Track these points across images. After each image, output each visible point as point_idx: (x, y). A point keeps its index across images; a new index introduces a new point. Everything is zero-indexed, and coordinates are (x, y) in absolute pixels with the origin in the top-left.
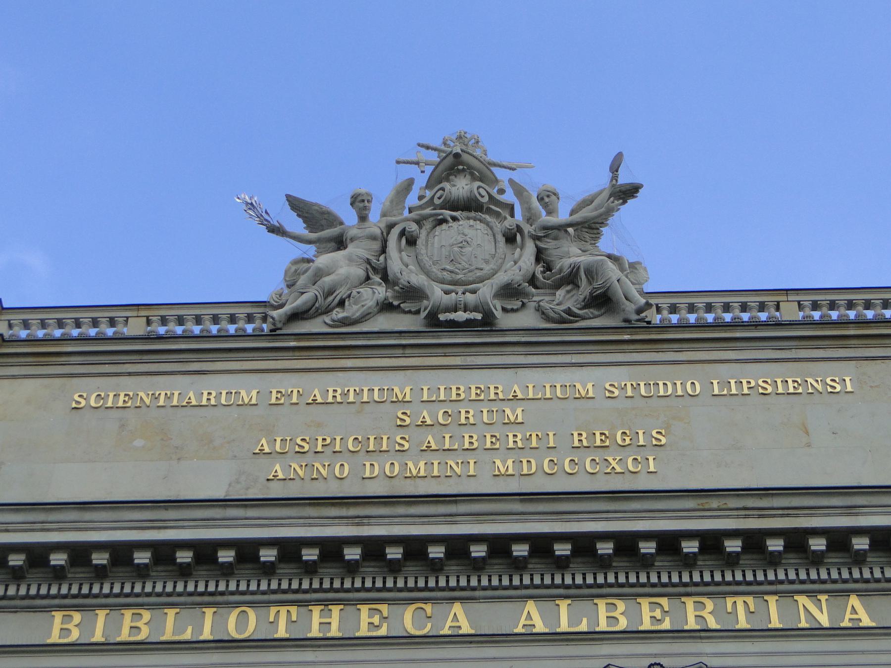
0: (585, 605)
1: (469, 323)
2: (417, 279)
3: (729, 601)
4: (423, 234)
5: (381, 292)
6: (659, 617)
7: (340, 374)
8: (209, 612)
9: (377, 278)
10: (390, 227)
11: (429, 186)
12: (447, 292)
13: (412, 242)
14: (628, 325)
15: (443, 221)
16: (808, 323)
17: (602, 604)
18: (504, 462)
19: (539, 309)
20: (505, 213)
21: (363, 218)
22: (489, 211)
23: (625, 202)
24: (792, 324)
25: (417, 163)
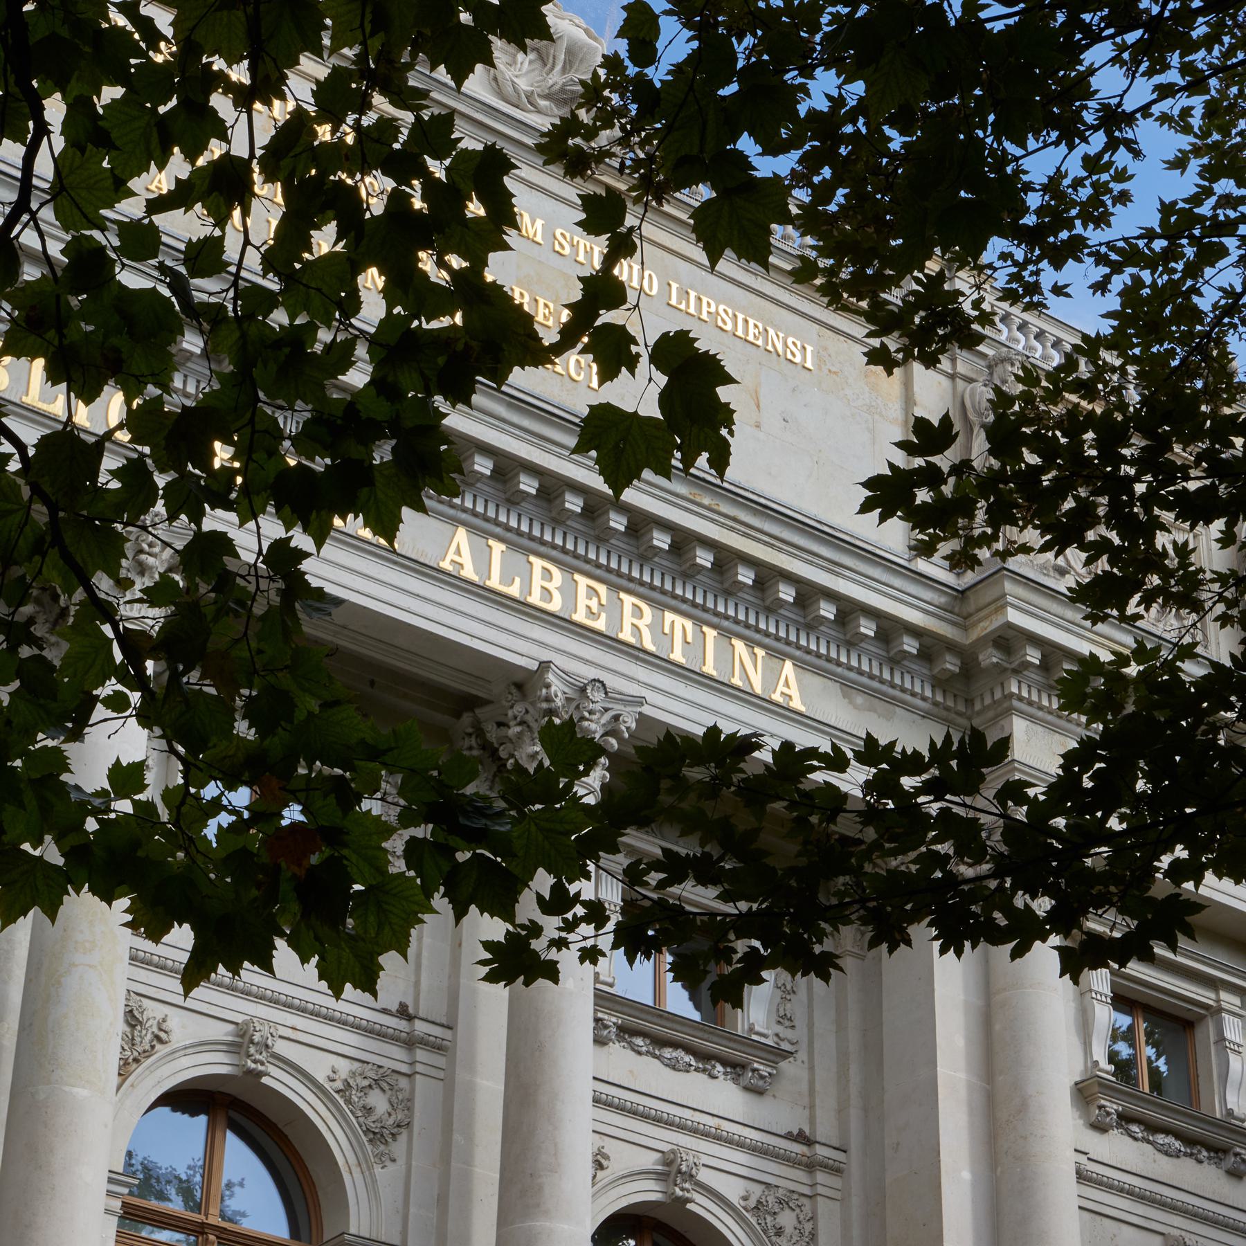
0: (519, 558)
6: (595, 610)
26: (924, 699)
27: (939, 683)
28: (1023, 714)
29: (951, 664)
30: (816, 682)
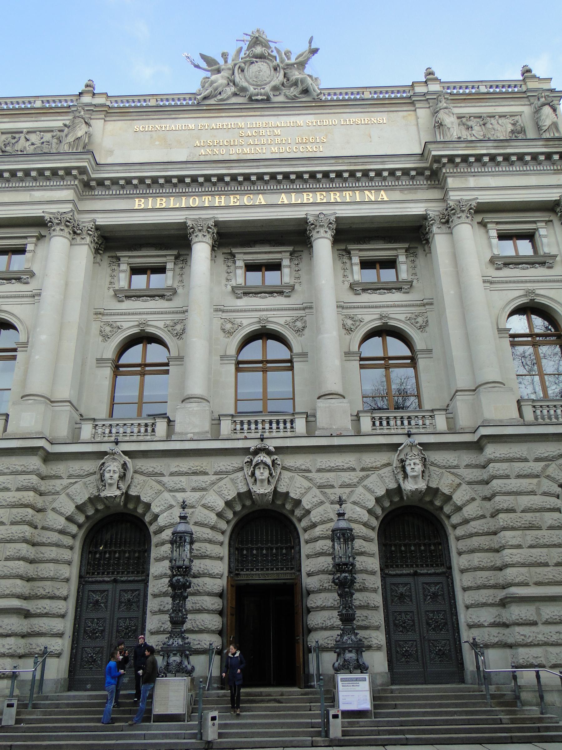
0: (300, 195)
1: (262, 100)
2: (245, 84)
3: (344, 193)
4: (246, 67)
5: (233, 89)
7: (221, 119)
8: (184, 198)
9: (231, 84)
10: (235, 65)
11: (248, 50)
12: (255, 89)
13: (243, 71)
14: (314, 100)
15: (252, 63)
16: (373, 99)
17: (305, 194)
18: (274, 148)
19: (285, 95)
20: (274, 60)
21: (226, 62)
22: (268, 59)
23: (313, 55)
24: (367, 99)
25: (244, 41)
26: (425, 185)
27: (429, 178)
28: (450, 176)
29: (427, 173)
30: (390, 193)
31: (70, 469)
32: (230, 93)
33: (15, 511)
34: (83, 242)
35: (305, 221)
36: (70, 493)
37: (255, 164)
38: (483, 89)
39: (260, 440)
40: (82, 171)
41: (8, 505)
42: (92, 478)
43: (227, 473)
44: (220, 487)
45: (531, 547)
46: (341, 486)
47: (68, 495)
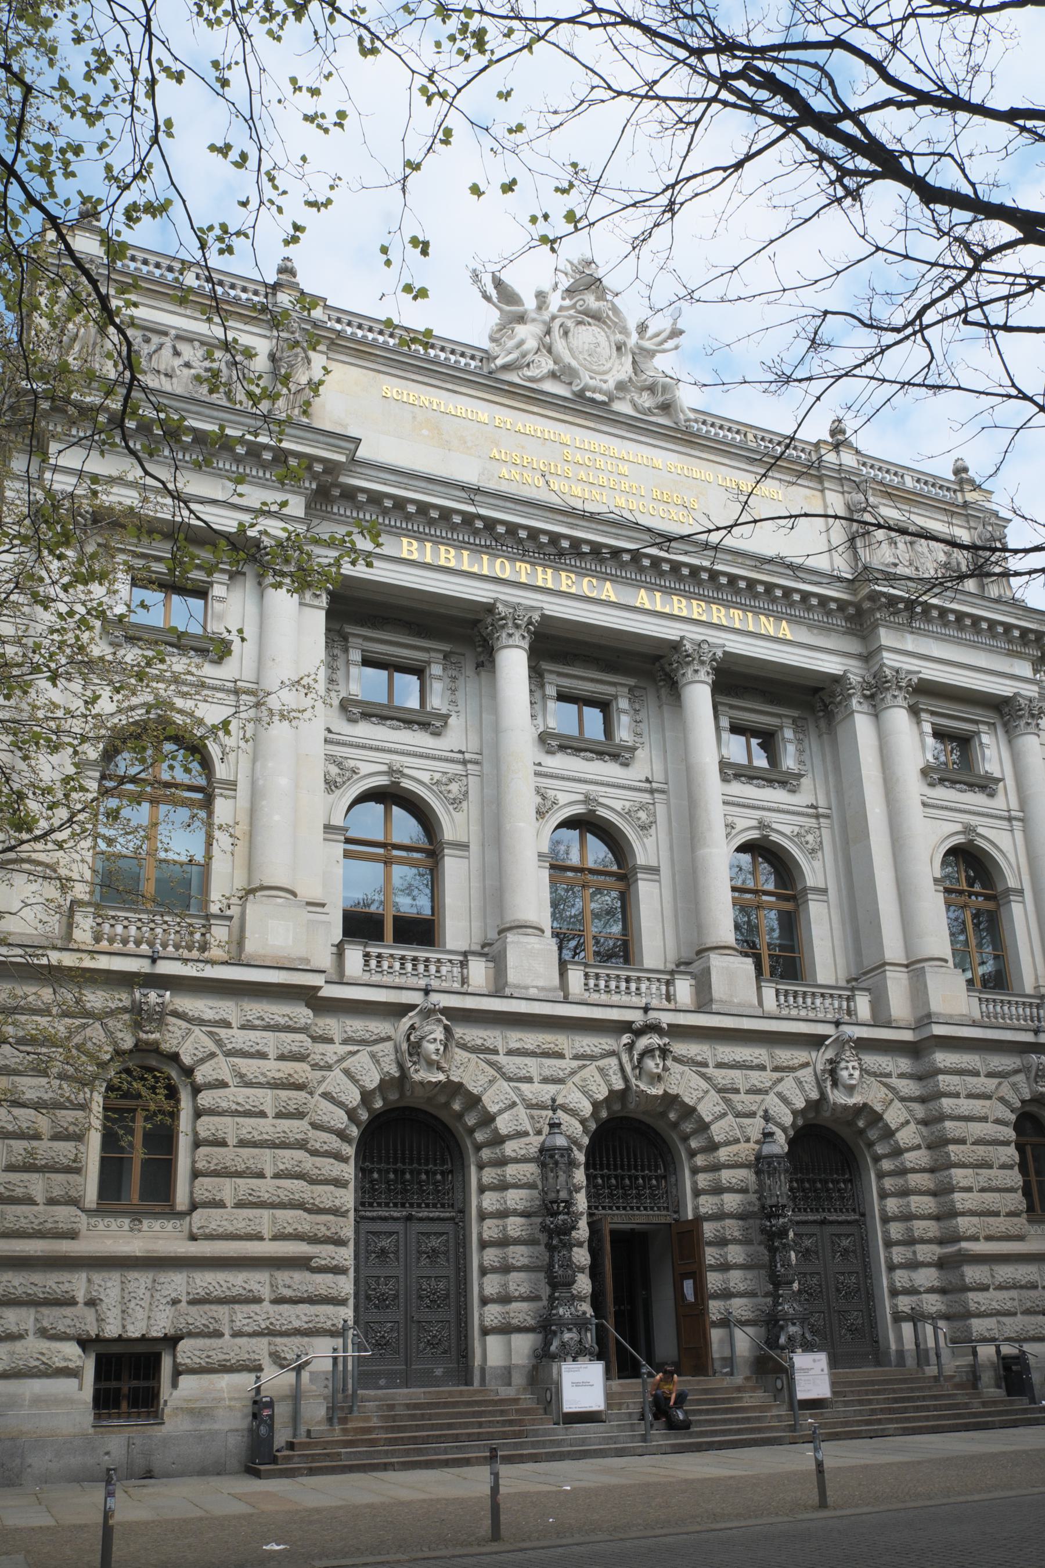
0: (666, 597)
2: (574, 363)
13: (566, 333)
19: (632, 401)
21: (539, 308)
27: (848, 619)
29: (851, 610)
31: (348, 1029)
32: (545, 371)
33: (284, 1094)
34: (316, 603)
35: (676, 646)
36: (353, 1069)
37: (614, 530)
38: (909, 483)
39: (641, 1012)
40: (331, 467)
41: (268, 1083)
42: (388, 1046)
43: (592, 1058)
44: (584, 1080)
45: (983, 1190)
46: (748, 1092)
47: (347, 1072)
